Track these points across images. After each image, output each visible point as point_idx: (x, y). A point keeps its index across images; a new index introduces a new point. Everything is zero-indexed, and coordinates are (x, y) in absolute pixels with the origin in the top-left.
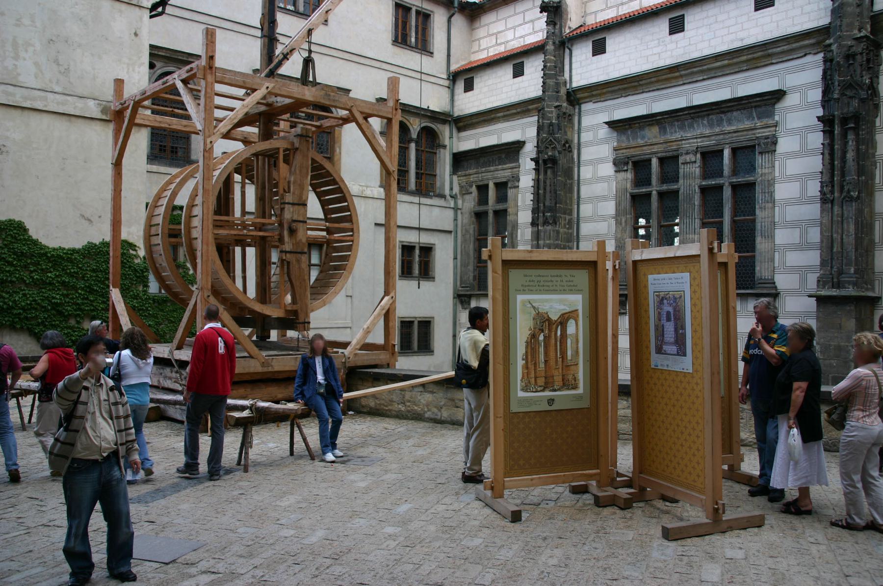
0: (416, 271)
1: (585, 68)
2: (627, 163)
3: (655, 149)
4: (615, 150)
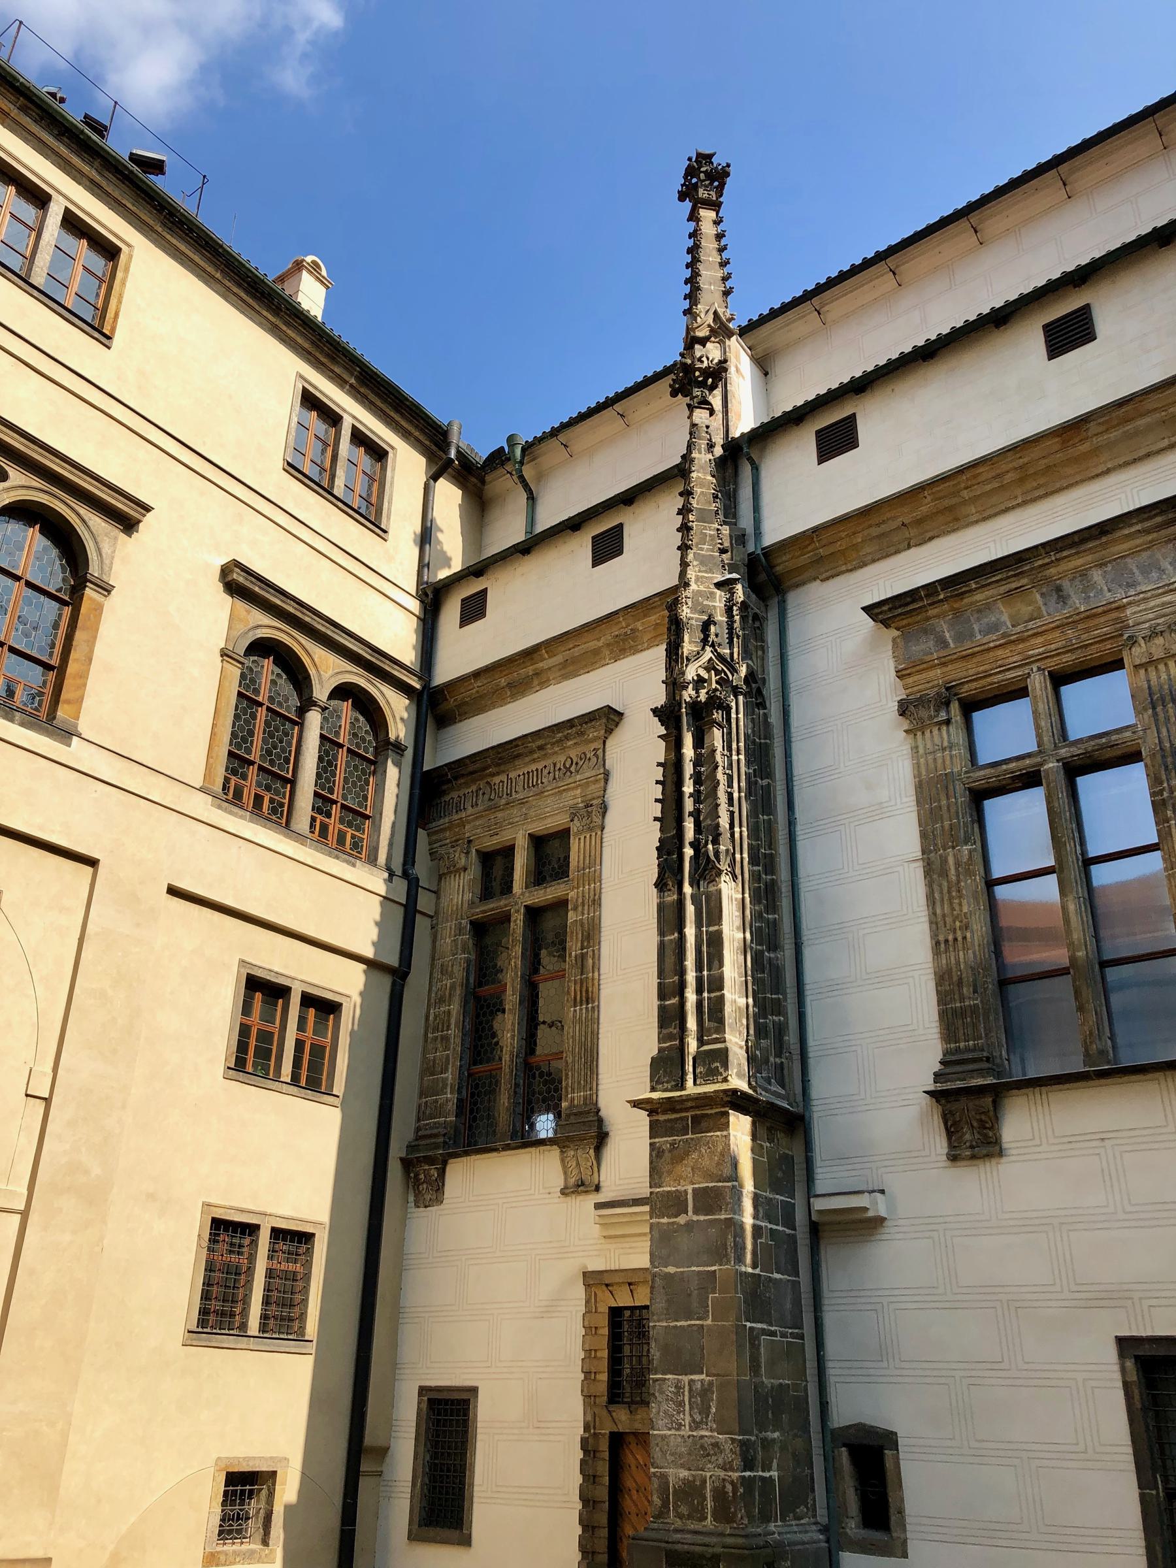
1: (800, 494)
2: (947, 704)
3: (1036, 647)
4: (901, 675)
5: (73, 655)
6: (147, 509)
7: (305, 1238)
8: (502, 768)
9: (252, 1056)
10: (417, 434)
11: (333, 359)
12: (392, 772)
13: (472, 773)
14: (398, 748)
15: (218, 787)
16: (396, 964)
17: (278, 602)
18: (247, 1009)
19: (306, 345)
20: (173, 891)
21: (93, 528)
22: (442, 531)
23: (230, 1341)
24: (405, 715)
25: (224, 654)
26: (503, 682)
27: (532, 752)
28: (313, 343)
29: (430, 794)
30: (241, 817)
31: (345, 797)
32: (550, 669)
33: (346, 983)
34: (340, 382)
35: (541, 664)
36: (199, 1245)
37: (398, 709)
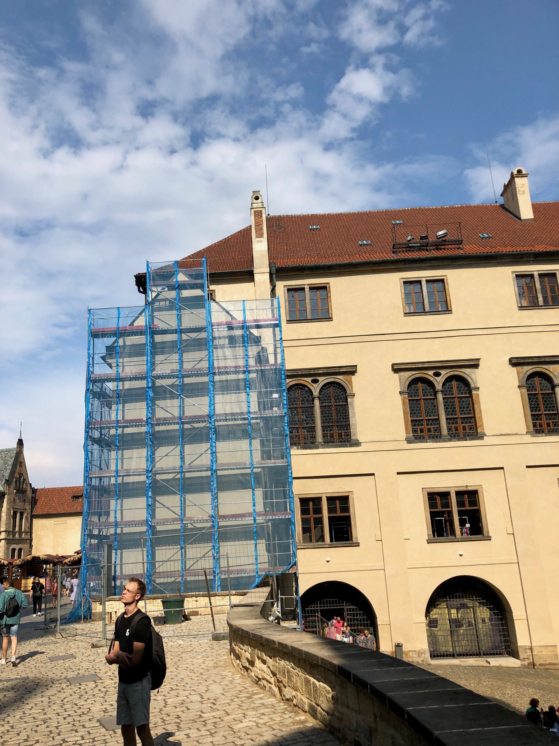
5: (476, 413)
6: (479, 359)
15: (532, 429)
19: (512, 260)
20: (528, 467)
25: (519, 387)
28: (512, 258)
34: (528, 263)
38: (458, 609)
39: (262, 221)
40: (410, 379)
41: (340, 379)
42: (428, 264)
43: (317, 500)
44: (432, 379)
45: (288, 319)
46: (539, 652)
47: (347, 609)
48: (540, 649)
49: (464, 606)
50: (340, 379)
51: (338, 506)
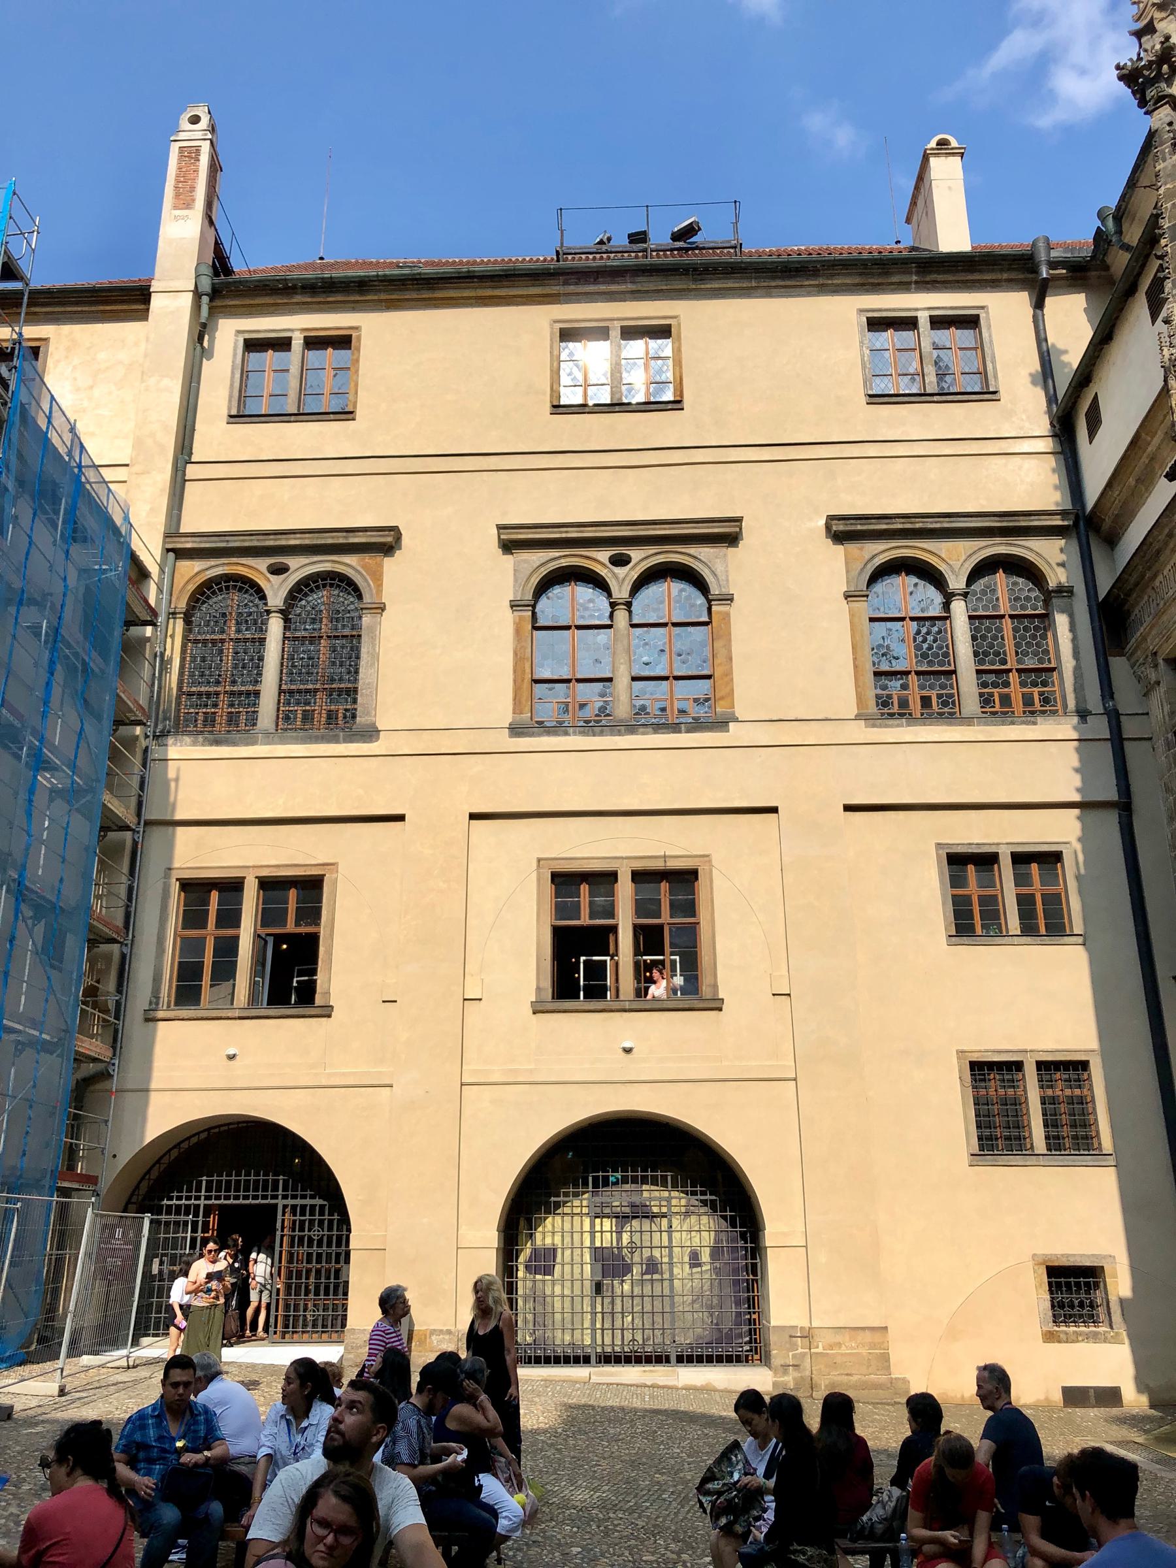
0: (1013, 922)
6: (738, 520)
7: (1084, 1065)
8: (1154, 569)
9: (970, 920)
10: (1005, 276)
11: (887, 274)
12: (1061, 621)
13: (1137, 584)
14: (1065, 591)
15: (872, 708)
16: (1116, 798)
17: (884, 527)
18: (956, 881)
19: (857, 280)
20: (848, 808)
21: (702, 557)
22: (1066, 352)
23: (1019, 1160)
24: (1063, 557)
25: (847, 596)
26: (1132, 481)
27: (1166, 544)
28: (861, 274)
29: (1113, 622)
30: (898, 726)
31: (1019, 662)
32: (1159, 448)
33: (1062, 831)
35: (1150, 449)
36: (962, 1085)
37: (1052, 556)
38: (622, 1219)
39: (196, 171)
40: (544, 571)
41: (349, 564)
42: (630, 287)
43: (232, 887)
44: (603, 572)
45: (234, 412)
46: (831, 1347)
47: (285, 1207)
48: (831, 1338)
49: (641, 1212)
50: (349, 564)
51: (292, 906)
